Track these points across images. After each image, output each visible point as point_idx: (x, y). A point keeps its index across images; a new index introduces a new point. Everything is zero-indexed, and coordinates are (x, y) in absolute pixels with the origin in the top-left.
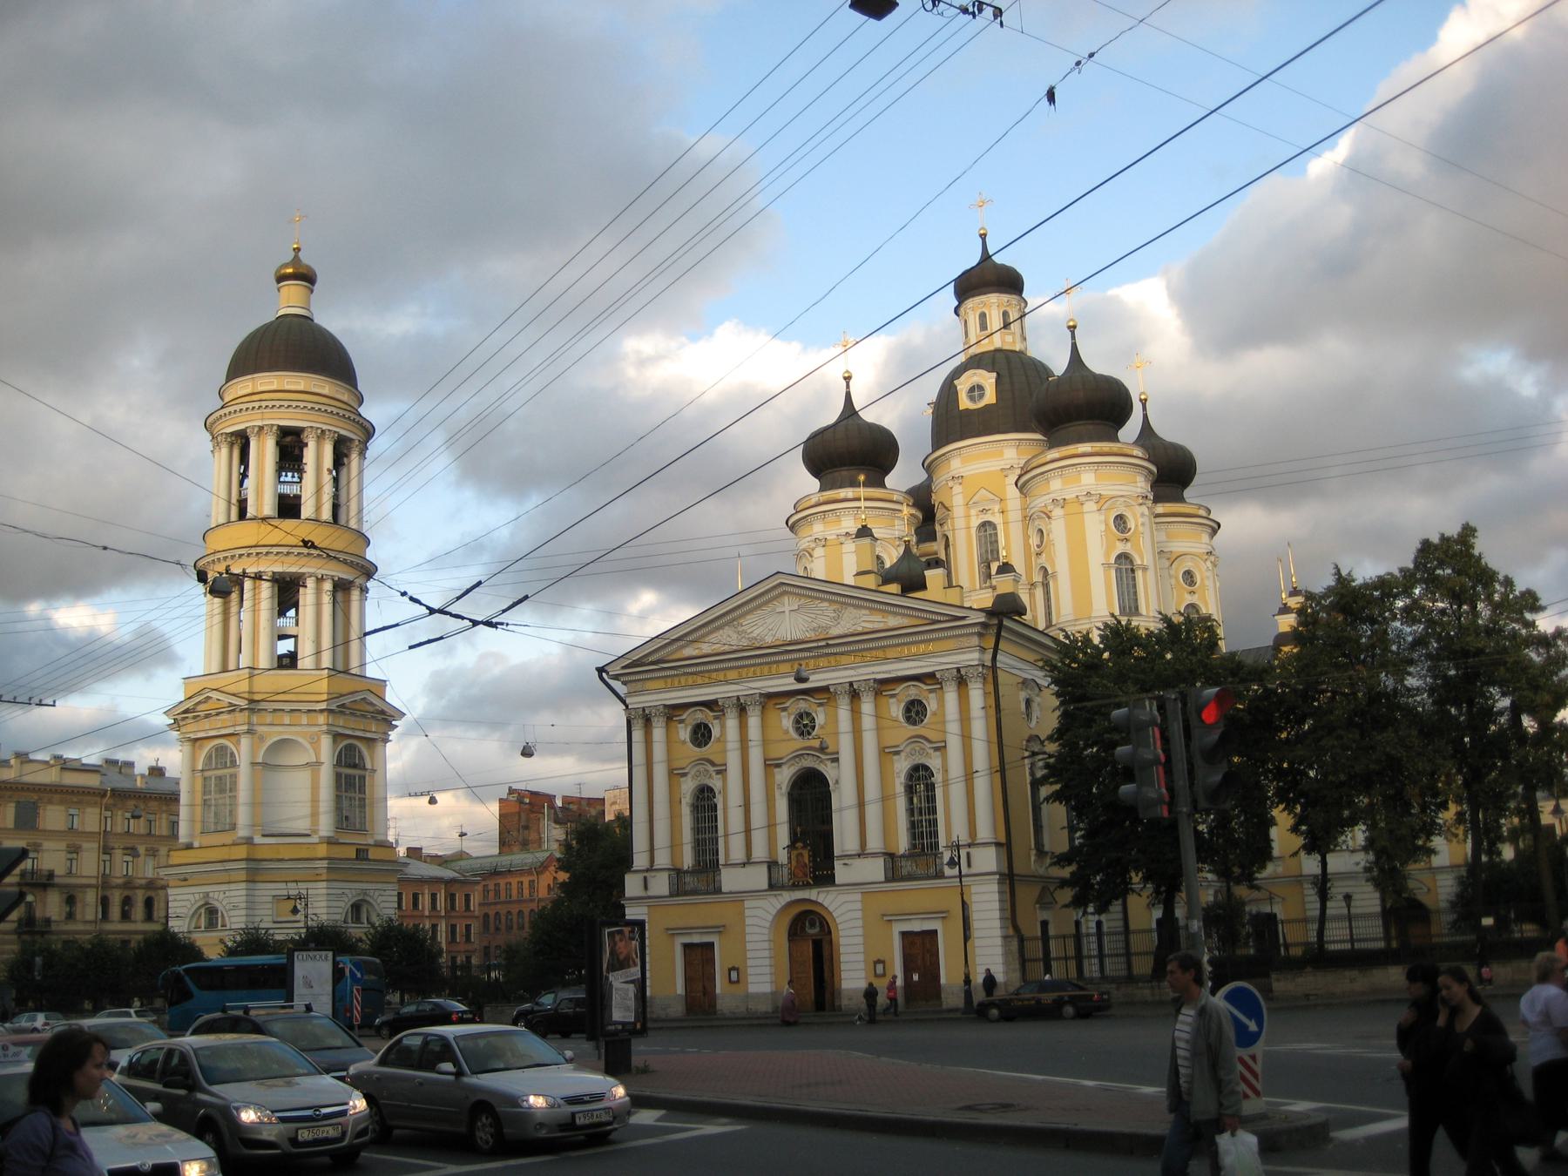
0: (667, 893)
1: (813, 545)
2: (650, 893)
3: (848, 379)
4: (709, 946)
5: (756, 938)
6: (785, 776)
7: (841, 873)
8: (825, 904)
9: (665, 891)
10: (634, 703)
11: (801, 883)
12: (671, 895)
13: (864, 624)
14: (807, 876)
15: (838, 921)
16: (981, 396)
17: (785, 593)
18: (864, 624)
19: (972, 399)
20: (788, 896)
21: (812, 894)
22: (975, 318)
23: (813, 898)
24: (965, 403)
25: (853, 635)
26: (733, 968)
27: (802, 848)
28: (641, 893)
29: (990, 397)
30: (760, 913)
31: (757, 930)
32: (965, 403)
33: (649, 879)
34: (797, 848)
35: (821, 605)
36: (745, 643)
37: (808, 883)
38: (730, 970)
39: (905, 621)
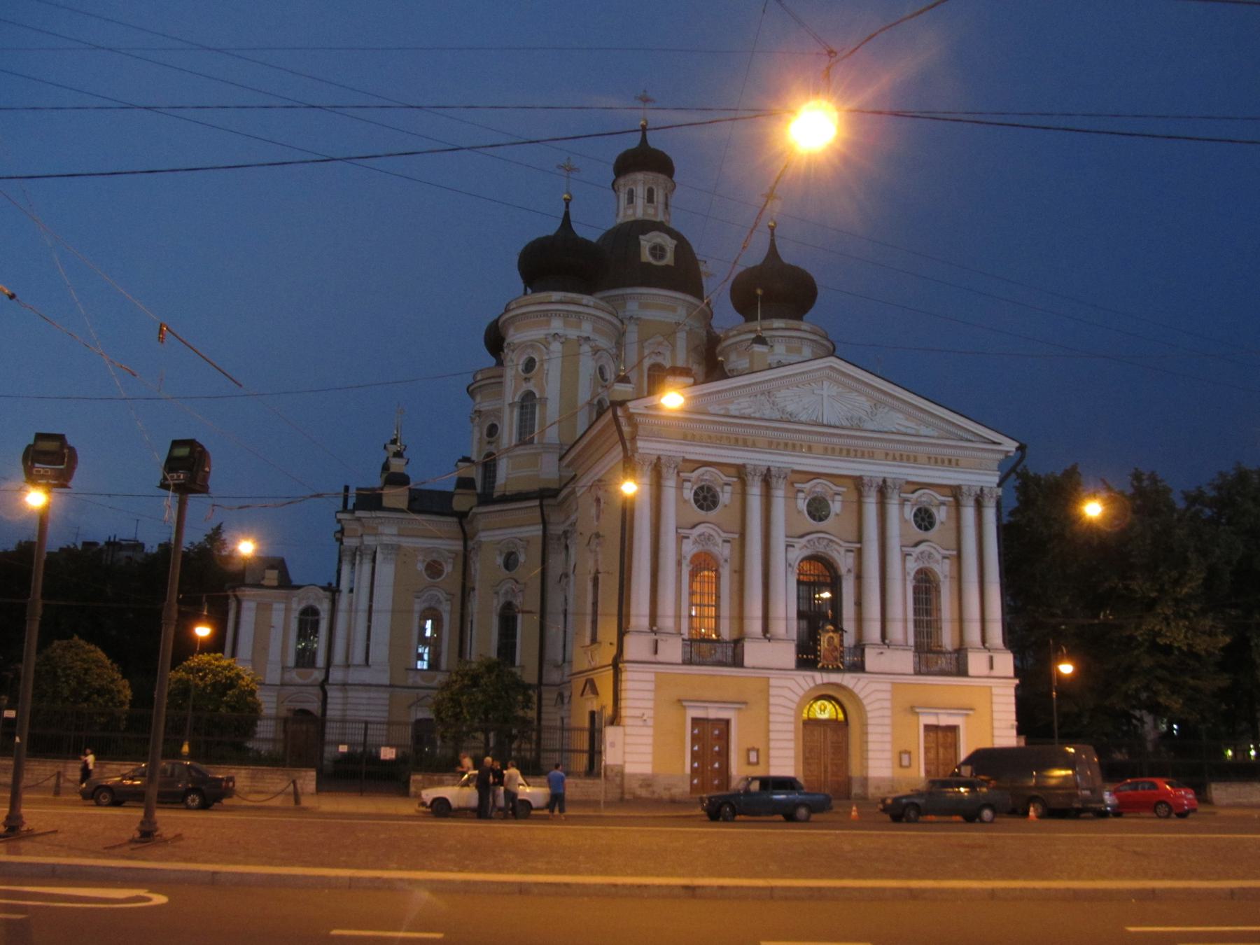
0: (680, 661)
1: (550, 339)
2: (660, 657)
3: (567, 202)
4: (953, 729)
5: (780, 718)
6: (797, 554)
7: (872, 659)
8: (856, 690)
9: (678, 658)
10: (643, 448)
11: (830, 667)
12: (684, 663)
13: (897, 426)
14: (836, 660)
15: (868, 708)
16: (662, 257)
17: (829, 378)
18: (897, 426)
19: (654, 256)
20: (820, 678)
21: (847, 679)
22: (644, 189)
23: (845, 683)
24: (646, 256)
25: (899, 433)
26: (753, 749)
27: (833, 631)
28: (646, 655)
29: (669, 259)
30: (787, 693)
31: (781, 710)
32: (646, 256)
33: (659, 641)
34: (828, 631)
35: (857, 398)
36: (777, 415)
37: (838, 667)
38: (749, 750)
39: (935, 434)
